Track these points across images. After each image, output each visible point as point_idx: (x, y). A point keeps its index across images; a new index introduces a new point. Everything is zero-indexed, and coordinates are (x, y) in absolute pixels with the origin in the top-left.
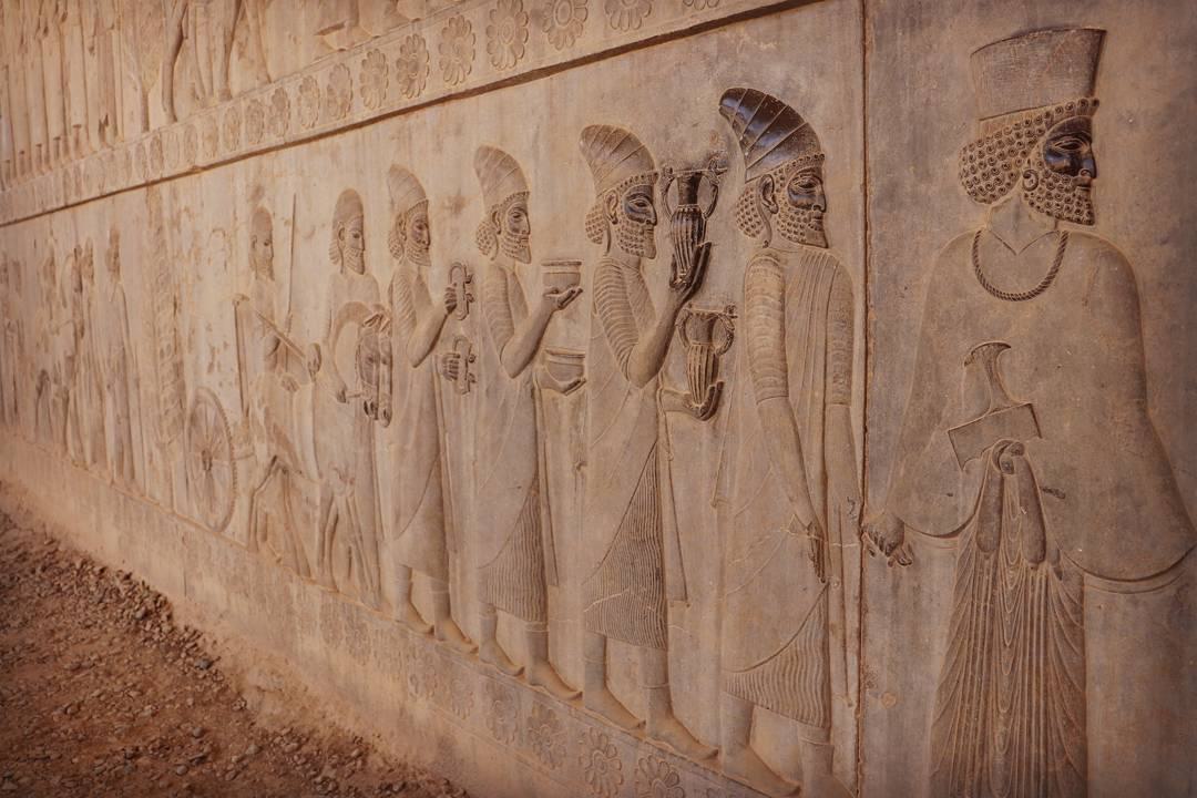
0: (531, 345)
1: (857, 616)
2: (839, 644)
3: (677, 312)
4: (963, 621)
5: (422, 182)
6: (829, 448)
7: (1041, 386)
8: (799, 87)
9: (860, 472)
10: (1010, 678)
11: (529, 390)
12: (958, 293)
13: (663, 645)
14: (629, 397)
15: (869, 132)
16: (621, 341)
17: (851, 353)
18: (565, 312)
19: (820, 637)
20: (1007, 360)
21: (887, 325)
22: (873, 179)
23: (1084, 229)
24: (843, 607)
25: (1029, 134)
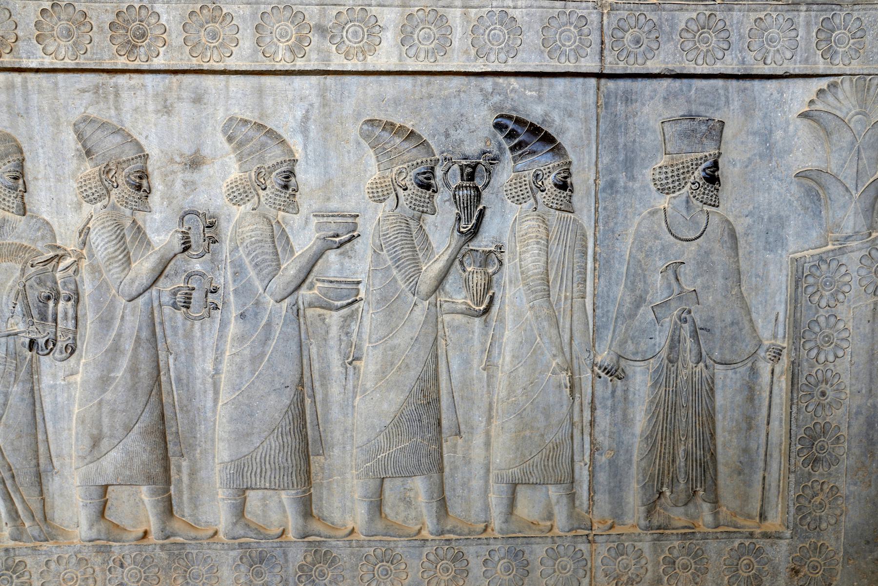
0: (302, 276)
1: (589, 413)
2: (579, 432)
3: (460, 249)
4: (659, 400)
5: (136, 136)
6: (575, 323)
7: (699, 281)
8: (554, 121)
9: (591, 334)
10: (686, 421)
11: (296, 311)
12: (657, 238)
13: (441, 470)
14: (415, 308)
15: (599, 152)
16: (411, 270)
17: (586, 269)
18: (339, 251)
19: (570, 430)
20: (682, 270)
21: (607, 254)
22: (601, 177)
23: (714, 209)
24: (582, 410)
25: (697, 164)
